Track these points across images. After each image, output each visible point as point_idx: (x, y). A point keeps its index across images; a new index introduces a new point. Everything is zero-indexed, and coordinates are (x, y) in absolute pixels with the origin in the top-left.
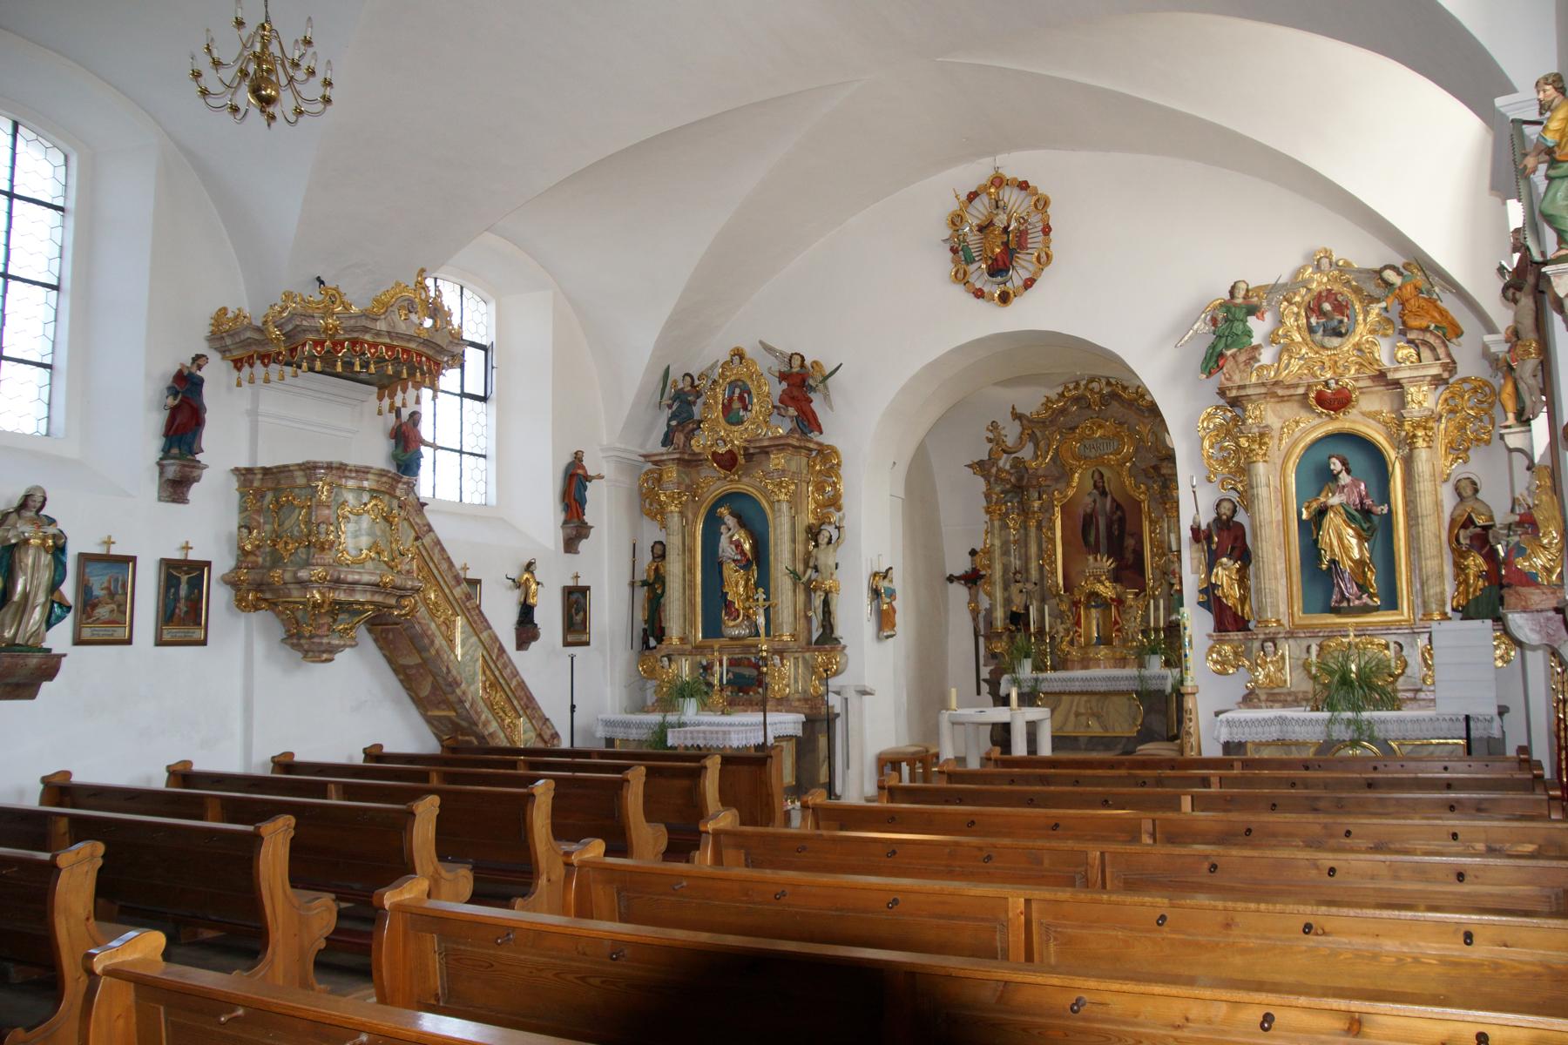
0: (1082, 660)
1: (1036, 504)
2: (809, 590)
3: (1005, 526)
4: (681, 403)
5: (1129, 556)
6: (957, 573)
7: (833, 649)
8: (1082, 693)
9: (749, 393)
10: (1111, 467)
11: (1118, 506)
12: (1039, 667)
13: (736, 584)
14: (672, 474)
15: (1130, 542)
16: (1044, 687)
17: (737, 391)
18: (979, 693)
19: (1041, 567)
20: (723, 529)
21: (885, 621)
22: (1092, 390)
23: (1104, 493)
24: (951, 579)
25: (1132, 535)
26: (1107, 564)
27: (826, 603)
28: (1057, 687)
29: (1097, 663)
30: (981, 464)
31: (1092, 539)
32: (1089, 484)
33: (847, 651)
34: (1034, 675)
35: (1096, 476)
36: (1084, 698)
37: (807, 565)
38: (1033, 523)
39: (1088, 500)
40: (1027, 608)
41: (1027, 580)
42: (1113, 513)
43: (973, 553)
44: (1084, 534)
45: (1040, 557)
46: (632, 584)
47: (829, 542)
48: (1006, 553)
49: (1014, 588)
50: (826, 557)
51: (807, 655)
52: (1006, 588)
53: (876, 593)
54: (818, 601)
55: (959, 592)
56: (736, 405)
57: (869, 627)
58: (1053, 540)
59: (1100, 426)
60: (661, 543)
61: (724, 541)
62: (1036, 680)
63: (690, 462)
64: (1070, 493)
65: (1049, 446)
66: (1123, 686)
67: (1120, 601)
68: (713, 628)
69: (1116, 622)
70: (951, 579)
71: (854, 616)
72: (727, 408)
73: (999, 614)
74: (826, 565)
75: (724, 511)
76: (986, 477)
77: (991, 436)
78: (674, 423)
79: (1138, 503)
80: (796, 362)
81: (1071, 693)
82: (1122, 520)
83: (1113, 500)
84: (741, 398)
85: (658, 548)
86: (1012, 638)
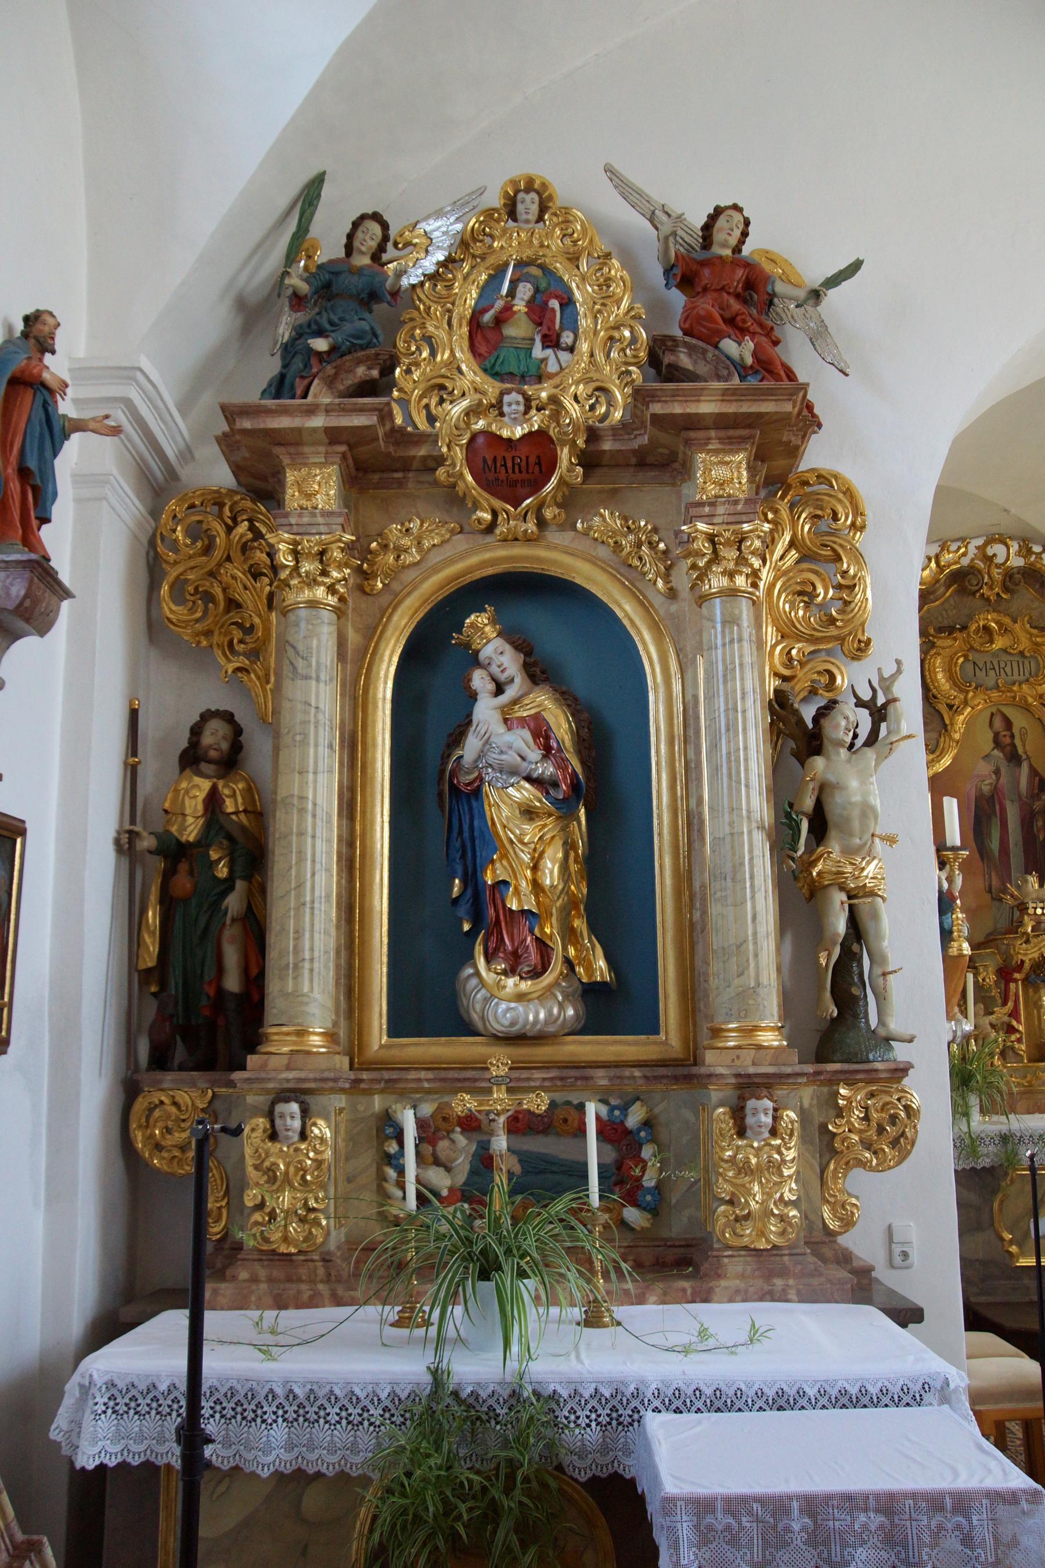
2: (801, 895)
4: (331, 310)
9: (567, 302)
13: (532, 855)
14: (316, 488)
17: (525, 291)
20: (479, 680)
22: (989, 559)
23: (1014, 758)
32: (985, 740)
35: (998, 723)
39: (984, 769)
46: (126, 845)
56: (518, 329)
59: (1005, 630)
60: (228, 717)
61: (486, 711)
63: (380, 468)
68: (427, 1001)
72: (484, 334)
74: (867, 811)
75: (481, 624)
78: (321, 345)
80: (725, 235)
83: (1034, 772)
84: (538, 311)
85: (215, 736)
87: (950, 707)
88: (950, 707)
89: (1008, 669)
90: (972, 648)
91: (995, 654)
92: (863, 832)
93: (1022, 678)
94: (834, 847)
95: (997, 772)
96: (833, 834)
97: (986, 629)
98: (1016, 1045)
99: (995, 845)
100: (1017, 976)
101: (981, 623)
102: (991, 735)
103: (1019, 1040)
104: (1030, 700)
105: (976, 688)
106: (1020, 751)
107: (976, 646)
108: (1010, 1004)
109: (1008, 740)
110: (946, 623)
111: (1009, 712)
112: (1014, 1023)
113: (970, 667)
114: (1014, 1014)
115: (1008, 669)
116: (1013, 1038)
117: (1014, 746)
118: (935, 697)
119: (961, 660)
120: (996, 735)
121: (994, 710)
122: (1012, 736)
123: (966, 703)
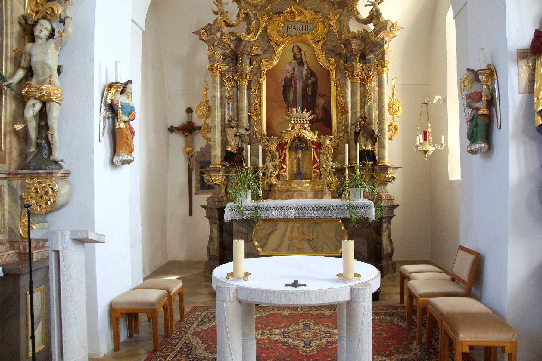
0: (287, 190)
1: (248, 69)
3: (222, 84)
5: (320, 112)
6: (177, 124)
7: (49, 175)
8: (297, 220)
10: (307, 43)
11: (312, 74)
12: (255, 197)
15: (321, 101)
16: (264, 215)
18: (191, 214)
19: (250, 117)
21: (119, 141)
23: (301, 63)
24: (171, 129)
25: (323, 96)
26: (307, 116)
27: (43, 115)
28: (274, 215)
29: (301, 194)
30: (209, 29)
31: (291, 98)
33: (71, 178)
34: (255, 203)
35: (296, 50)
36: (297, 224)
37: (18, 66)
38: (245, 83)
39: (289, 68)
40: (240, 150)
41: (238, 126)
42: (308, 78)
43: (189, 111)
44: (286, 93)
45: (249, 110)
47: (52, 35)
48: (223, 106)
49: (231, 132)
50: (45, 54)
51: (17, 183)
52: (223, 133)
53: (112, 108)
54: (32, 110)
55: (178, 140)
57: (101, 148)
58: (260, 97)
59: (301, 13)
62: (257, 208)
64: (276, 62)
65: (258, 25)
66: (334, 214)
67: (319, 146)
69: (315, 161)
70: (171, 129)
71: (79, 133)
73: (217, 153)
74: (44, 65)
76: (210, 43)
77: (217, 10)
79: (328, 73)
81: (287, 220)
82: (315, 85)
86: (226, 172)
87: (276, 43)
88: (276, 43)
89: (301, 28)
90: (287, 20)
91: (296, 23)
92: (44, 74)
93: (306, 32)
94: (34, 82)
95: (294, 69)
96: (35, 76)
97: (292, 12)
98: (283, 173)
99: (291, 98)
100: (285, 147)
101: (289, 10)
102: (292, 55)
103: (285, 172)
104: (309, 40)
105: (288, 36)
106: (304, 61)
107: (289, 19)
108: (282, 157)
109: (299, 56)
110: (278, 11)
111: (301, 45)
112: (283, 165)
113: (286, 28)
114: (284, 161)
115: (301, 28)
116: (282, 171)
117: (301, 58)
118: (270, 40)
119: (283, 25)
120: (295, 55)
121: (294, 44)
122: (301, 55)
123: (283, 42)
